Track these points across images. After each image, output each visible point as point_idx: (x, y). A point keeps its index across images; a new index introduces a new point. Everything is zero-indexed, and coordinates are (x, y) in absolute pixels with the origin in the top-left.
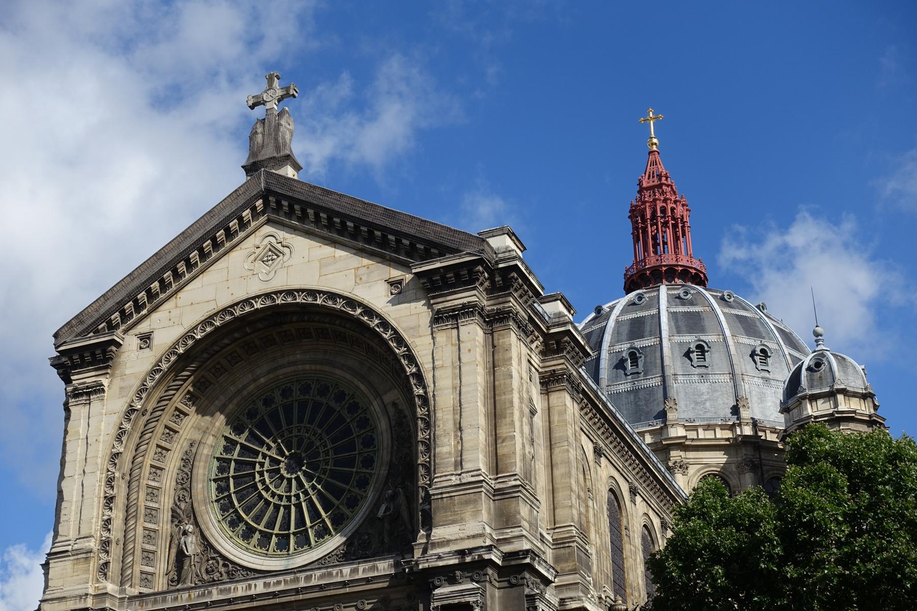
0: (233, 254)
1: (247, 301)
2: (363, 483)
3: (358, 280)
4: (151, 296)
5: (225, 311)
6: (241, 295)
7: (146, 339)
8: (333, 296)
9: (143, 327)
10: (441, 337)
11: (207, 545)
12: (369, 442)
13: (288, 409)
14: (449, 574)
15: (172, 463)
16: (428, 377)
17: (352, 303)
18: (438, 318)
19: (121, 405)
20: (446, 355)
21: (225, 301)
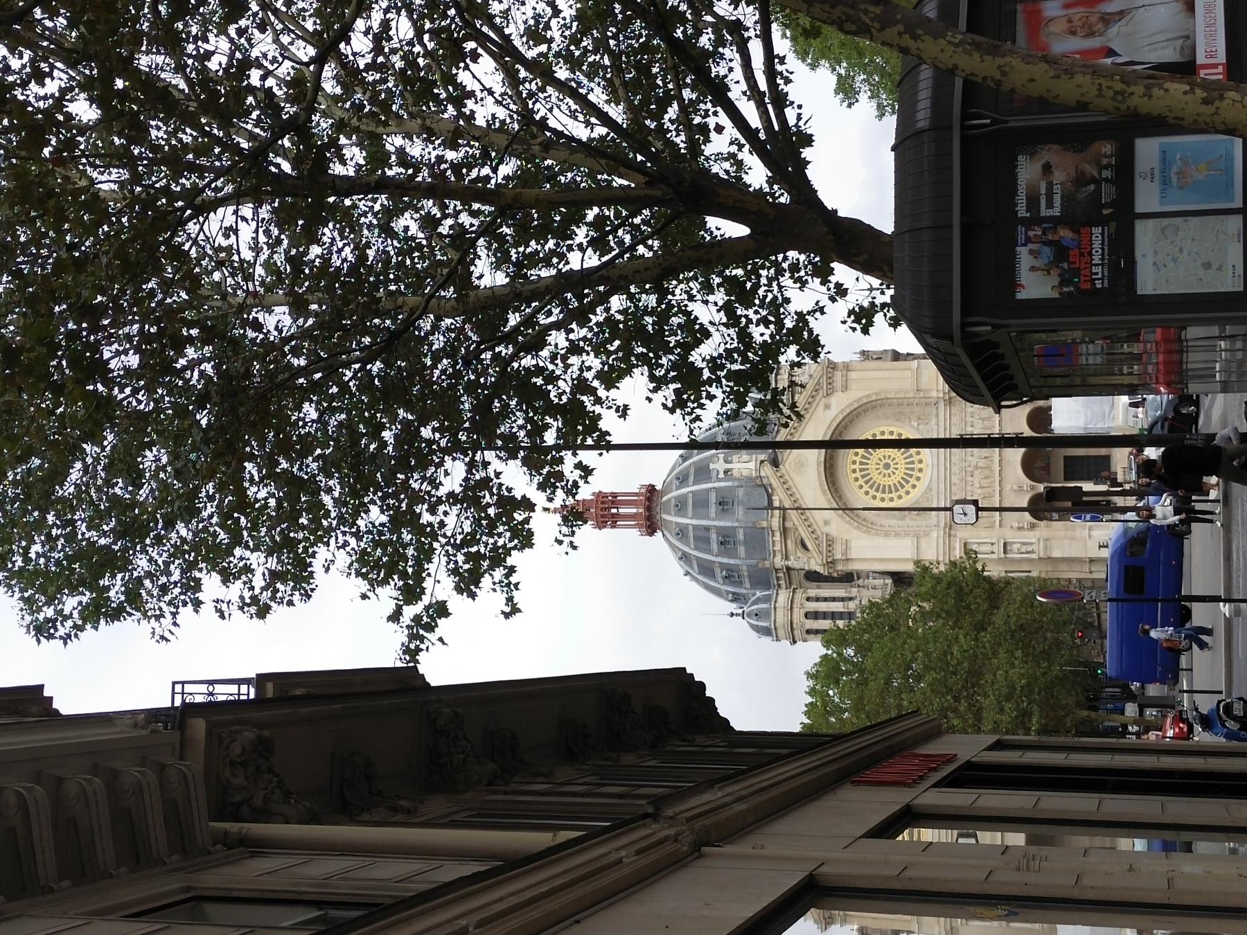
9: (821, 524)
19: (856, 532)
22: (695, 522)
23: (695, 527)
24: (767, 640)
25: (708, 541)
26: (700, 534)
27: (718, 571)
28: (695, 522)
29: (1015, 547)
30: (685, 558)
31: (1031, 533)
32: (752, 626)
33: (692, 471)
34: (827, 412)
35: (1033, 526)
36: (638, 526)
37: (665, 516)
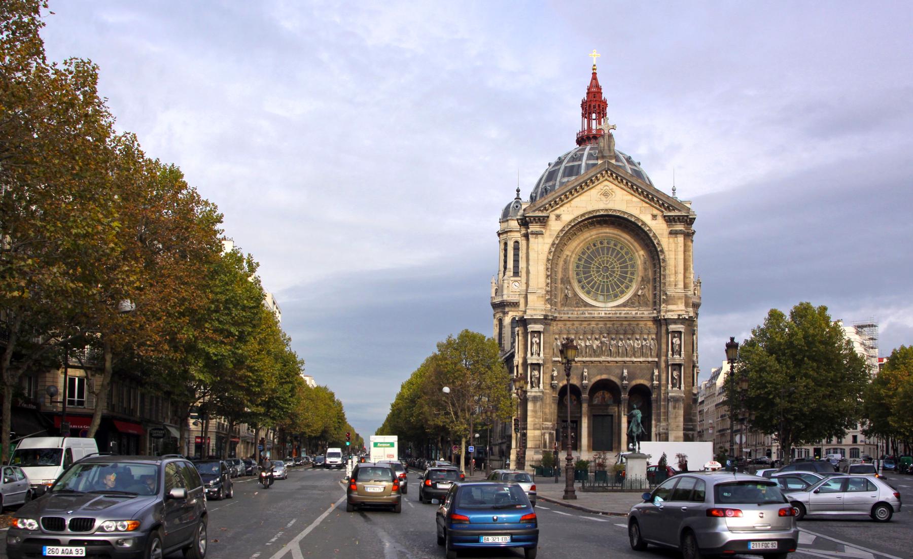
0: (592, 191)
1: (598, 210)
2: (631, 281)
3: (641, 212)
4: (562, 200)
5: (590, 212)
6: (596, 208)
7: (558, 217)
8: (632, 215)
9: (557, 212)
10: (671, 240)
11: (575, 295)
12: (633, 266)
13: (603, 249)
14: (675, 321)
15: (561, 263)
16: (666, 253)
17: (638, 219)
18: (671, 233)
20: (673, 246)
21: (590, 209)
22: (583, 164)
23: (579, 166)
24: (499, 215)
25: (570, 175)
26: (575, 170)
27: (551, 183)
28: (583, 164)
29: (536, 373)
30: (560, 161)
31: (548, 387)
32: (510, 204)
33: (620, 164)
34: (650, 217)
35: (553, 387)
36: (583, 131)
37: (588, 147)
